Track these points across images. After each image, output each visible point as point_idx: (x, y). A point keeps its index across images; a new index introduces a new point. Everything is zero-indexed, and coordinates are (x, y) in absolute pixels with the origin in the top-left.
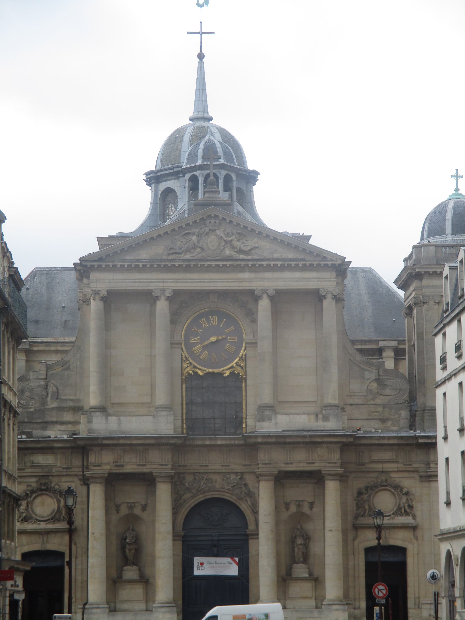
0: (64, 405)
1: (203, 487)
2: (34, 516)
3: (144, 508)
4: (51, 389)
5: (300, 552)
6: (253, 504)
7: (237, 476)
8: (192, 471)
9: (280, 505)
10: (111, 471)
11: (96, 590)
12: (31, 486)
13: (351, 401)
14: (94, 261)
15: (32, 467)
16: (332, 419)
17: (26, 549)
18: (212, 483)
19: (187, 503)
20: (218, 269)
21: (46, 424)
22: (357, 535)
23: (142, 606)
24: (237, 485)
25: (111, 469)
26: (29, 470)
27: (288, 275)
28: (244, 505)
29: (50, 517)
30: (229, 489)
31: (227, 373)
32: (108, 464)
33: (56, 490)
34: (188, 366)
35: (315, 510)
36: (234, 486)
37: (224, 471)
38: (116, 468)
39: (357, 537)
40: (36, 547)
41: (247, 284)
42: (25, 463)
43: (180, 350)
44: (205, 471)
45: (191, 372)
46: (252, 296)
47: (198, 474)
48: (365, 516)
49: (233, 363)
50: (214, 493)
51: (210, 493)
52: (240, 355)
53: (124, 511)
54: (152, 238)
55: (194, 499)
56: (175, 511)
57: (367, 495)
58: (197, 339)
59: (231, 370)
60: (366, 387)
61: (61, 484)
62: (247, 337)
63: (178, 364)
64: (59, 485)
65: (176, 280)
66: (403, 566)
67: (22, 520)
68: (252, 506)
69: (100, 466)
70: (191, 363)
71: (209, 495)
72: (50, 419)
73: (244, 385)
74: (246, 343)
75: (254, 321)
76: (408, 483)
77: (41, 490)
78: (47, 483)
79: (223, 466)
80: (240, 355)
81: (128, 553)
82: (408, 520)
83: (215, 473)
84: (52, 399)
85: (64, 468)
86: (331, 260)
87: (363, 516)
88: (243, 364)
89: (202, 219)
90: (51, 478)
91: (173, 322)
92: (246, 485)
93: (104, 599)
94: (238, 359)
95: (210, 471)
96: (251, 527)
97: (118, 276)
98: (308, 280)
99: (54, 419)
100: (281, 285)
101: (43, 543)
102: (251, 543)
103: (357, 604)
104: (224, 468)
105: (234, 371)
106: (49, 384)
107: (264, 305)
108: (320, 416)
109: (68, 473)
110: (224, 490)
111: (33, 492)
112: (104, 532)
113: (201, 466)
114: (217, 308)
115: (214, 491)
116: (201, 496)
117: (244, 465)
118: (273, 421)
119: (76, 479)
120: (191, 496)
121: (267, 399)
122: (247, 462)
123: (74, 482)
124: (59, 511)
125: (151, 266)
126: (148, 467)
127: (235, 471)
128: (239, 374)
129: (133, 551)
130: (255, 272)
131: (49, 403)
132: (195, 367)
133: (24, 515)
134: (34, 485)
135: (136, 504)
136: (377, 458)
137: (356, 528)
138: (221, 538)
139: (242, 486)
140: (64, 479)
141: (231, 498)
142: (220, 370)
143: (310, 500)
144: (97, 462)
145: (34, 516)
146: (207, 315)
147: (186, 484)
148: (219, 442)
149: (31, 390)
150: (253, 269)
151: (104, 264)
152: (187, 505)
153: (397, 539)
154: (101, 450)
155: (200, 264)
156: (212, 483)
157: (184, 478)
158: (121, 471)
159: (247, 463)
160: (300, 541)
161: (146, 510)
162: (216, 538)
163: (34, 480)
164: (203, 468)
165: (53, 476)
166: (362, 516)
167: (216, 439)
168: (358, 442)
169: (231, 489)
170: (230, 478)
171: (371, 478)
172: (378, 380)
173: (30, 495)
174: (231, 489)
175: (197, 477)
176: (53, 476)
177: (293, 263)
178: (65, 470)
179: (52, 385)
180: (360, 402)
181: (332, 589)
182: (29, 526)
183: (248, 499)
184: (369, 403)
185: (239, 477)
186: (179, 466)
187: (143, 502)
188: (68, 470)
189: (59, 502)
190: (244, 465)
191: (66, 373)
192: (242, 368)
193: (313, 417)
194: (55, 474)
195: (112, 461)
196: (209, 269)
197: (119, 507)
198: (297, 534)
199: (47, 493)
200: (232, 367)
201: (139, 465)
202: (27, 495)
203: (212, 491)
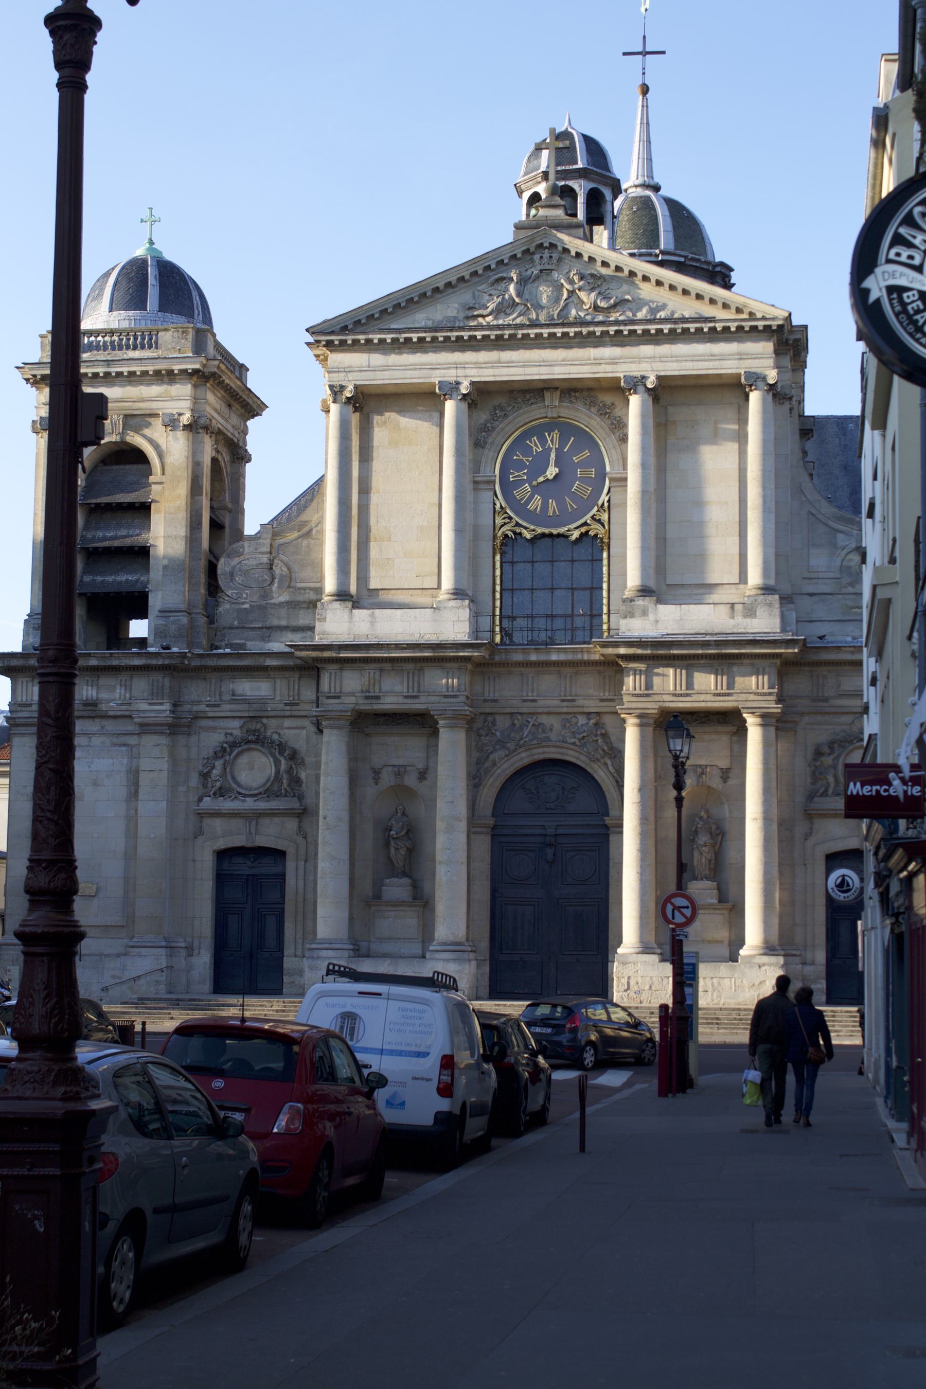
0: (300, 598)
2: (234, 786)
3: (423, 775)
4: (277, 571)
5: (704, 860)
7: (589, 719)
8: (508, 710)
10: (357, 707)
12: (231, 734)
13: (811, 589)
14: (332, 333)
15: (232, 701)
16: (760, 611)
17: (222, 844)
20: (554, 342)
21: (269, 631)
22: (811, 829)
23: (417, 949)
24: (588, 736)
25: (357, 704)
26: (227, 707)
27: (681, 349)
28: (602, 773)
29: (262, 790)
30: (574, 744)
31: (576, 535)
32: (352, 694)
33: (273, 742)
34: (505, 524)
35: (731, 782)
37: (565, 710)
38: (366, 701)
39: (811, 834)
41: (609, 368)
42: (220, 695)
43: (492, 493)
44: (532, 710)
45: (510, 534)
47: (519, 717)
48: (827, 795)
49: (587, 518)
50: (546, 749)
51: (541, 750)
52: (600, 502)
53: (387, 779)
54: (436, 290)
56: (475, 780)
57: (832, 757)
58: (523, 475)
59: (583, 530)
60: (838, 563)
61: (282, 732)
63: (487, 520)
64: (279, 734)
65: (478, 365)
67: (215, 794)
68: (615, 775)
69: (338, 697)
70: (510, 518)
71: (540, 754)
72: (275, 622)
73: (605, 555)
74: (611, 480)
75: (624, 439)
77: (249, 742)
78: (258, 731)
79: (563, 701)
80: (600, 502)
81: (394, 855)
83: (549, 713)
84: (279, 587)
85: (286, 704)
86: (764, 318)
87: (824, 794)
88: (605, 517)
89: (527, 252)
90: (265, 721)
91: (478, 444)
92: (605, 736)
93: (344, 934)
94: (596, 508)
95: (540, 710)
97: (377, 359)
98: (723, 357)
99: (284, 623)
100: (672, 369)
101: (250, 833)
103: (809, 956)
104: (565, 704)
105: (587, 532)
106: (276, 561)
108: (738, 608)
109: (294, 713)
110: (565, 745)
111: (233, 745)
112: (345, 816)
113: (524, 701)
114: (559, 417)
115: (548, 746)
116: (523, 755)
117: (602, 700)
118: (651, 617)
119: (306, 723)
120: (506, 756)
122: (607, 694)
123: (303, 728)
124: (278, 777)
125: (434, 339)
126: (423, 699)
127: (587, 710)
128: (596, 535)
129: (403, 851)
130: (622, 345)
131: (274, 595)
132: (517, 524)
133: (218, 784)
134: (237, 733)
135: (409, 768)
136: (851, 689)
137: (810, 816)
138: (560, 831)
139: (599, 738)
140: (287, 723)
141: (578, 758)
142: (562, 530)
143: (724, 763)
144: (333, 691)
145: (234, 786)
146: (540, 431)
147: (498, 734)
148: (554, 657)
149: (246, 573)
151: (350, 339)
152: (499, 771)
154: (341, 669)
155: (520, 333)
156: (544, 732)
157: (494, 723)
158: (375, 707)
159: (607, 695)
160: (703, 839)
161: (426, 779)
162: (551, 831)
163: (237, 723)
164: (528, 704)
165: (267, 717)
166: (822, 795)
167: (548, 652)
168: (814, 657)
169: (578, 743)
171: (841, 724)
173: (228, 750)
175: (516, 722)
176: (267, 717)
177: (692, 327)
178: (288, 708)
179: (281, 564)
180: (828, 590)
183: (609, 762)
184: (844, 591)
185: (592, 721)
186: (485, 701)
187: (421, 766)
188: (294, 708)
189: (277, 763)
190: (602, 700)
191: (305, 542)
192: (603, 525)
193: (724, 610)
194: (270, 714)
195: (360, 689)
196: (538, 342)
197: (379, 773)
198: (699, 826)
199: (259, 747)
200: (585, 524)
201: (406, 697)
202: (224, 750)
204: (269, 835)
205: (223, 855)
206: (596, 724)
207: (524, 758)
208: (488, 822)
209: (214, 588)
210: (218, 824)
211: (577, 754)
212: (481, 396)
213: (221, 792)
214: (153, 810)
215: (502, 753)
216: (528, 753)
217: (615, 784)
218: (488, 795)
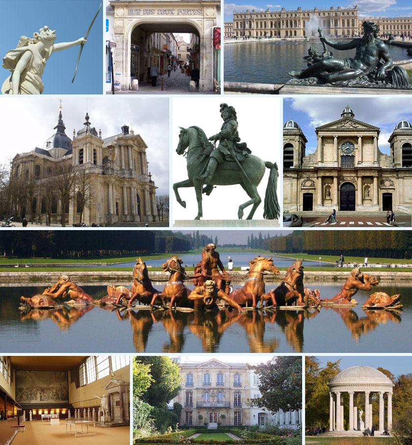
9: (363, 184)
11: (319, 201)
20: (349, 131)
40: (307, 192)
46: (357, 138)
62: (355, 147)
66: (391, 197)
71: (346, 181)
76: (392, 179)
82: (393, 187)
96: (356, 188)
102: (356, 192)
107: (360, 139)
121: (360, 160)
150: (357, 131)
153: (390, 191)
172: (385, 158)
181: (375, 202)
182: (304, 188)
196: (347, 131)
204: (310, 191)
205: (304, 194)
209: (302, 162)
210: (304, 190)
212: (339, 138)
213: (304, 186)
214: (295, 188)
218: (340, 187)
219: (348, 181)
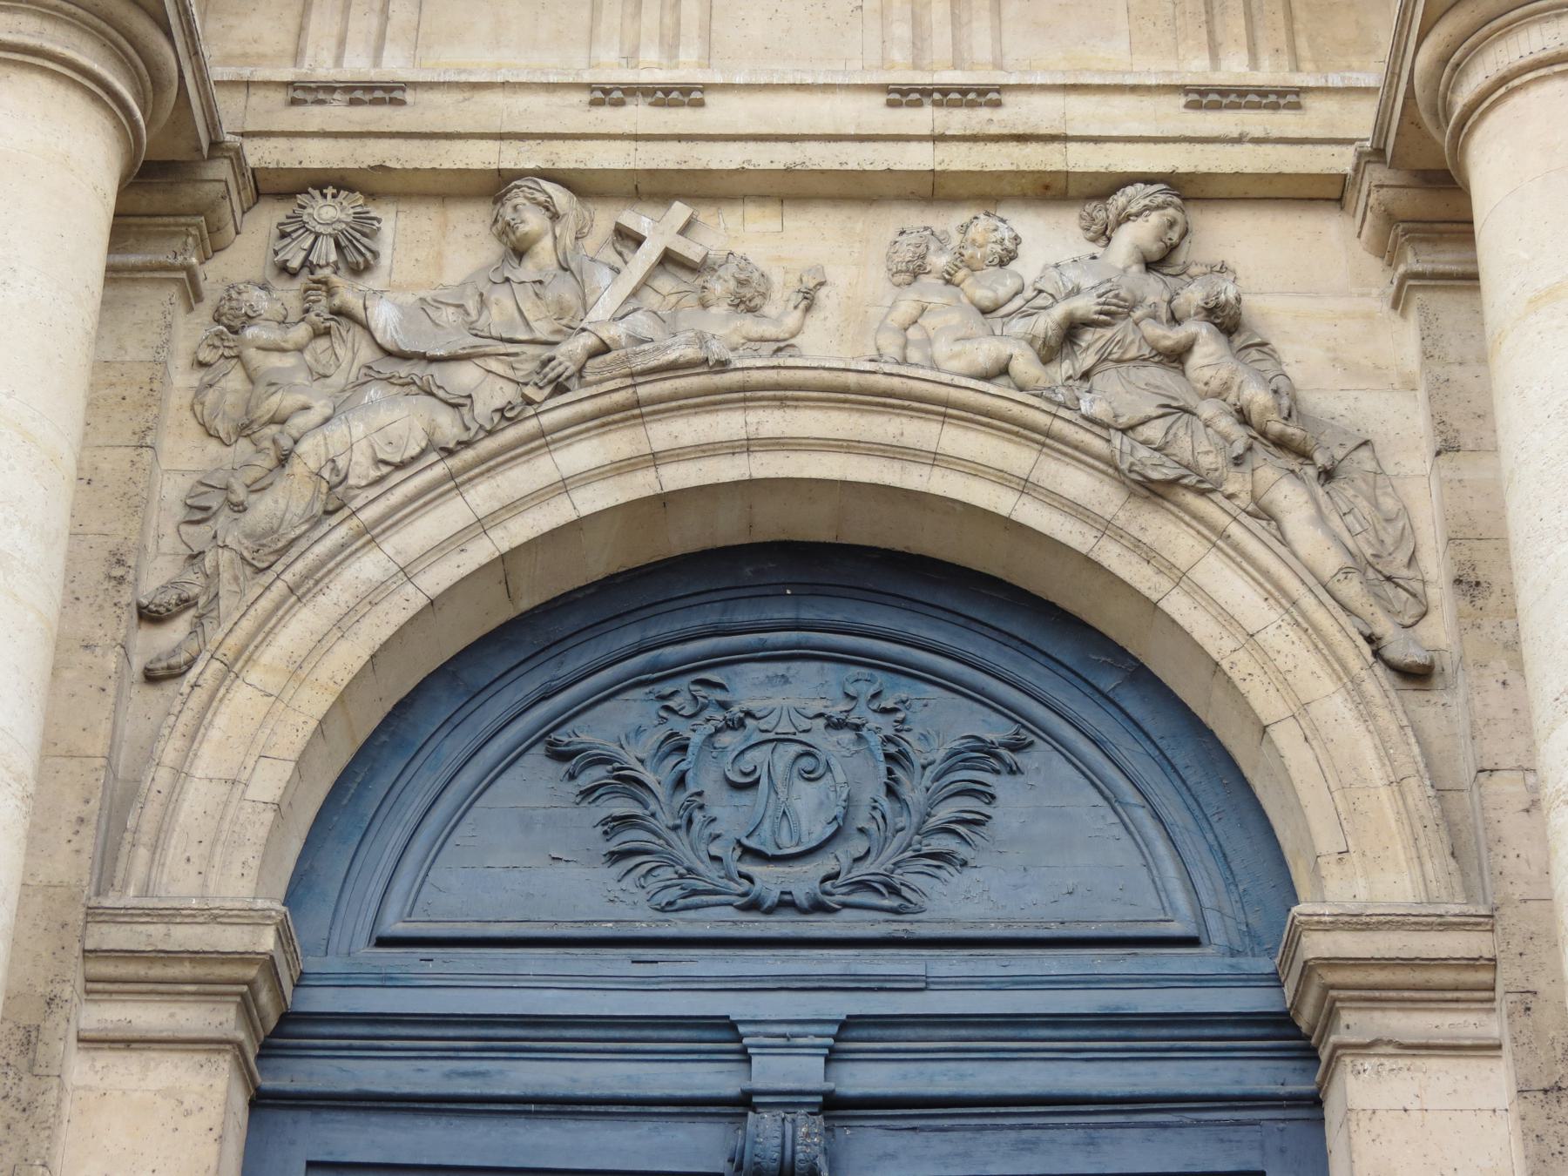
1: (612, 332)
6: (1358, 565)
7: (1104, 235)
18: (746, 303)
19: (369, 536)
36: (1072, 331)
37: (919, 158)
47: (560, 197)
50: (771, 422)
55: (482, 496)
68: (1352, 590)
71: (702, 452)
79: (902, 96)
92: (1226, 320)
104: (923, 118)
113: (606, 95)
115: (784, 395)
117: (1203, 97)
138: (861, 1079)
141: (1026, 487)
152: (369, 567)
157: (357, 257)
159: (1234, 70)
164: (639, 116)
170: (1006, 258)
174: (1025, 365)
175: (533, 221)
186: (303, 92)
190: (1203, 97)
203: (747, 395)
206: (1157, 262)
207: (579, 481)
208: (232, 939)
211: (1017, 457)
215: (400, 421)
216: (620, 443)
217: (1356, 656)
219: (819, 451)
